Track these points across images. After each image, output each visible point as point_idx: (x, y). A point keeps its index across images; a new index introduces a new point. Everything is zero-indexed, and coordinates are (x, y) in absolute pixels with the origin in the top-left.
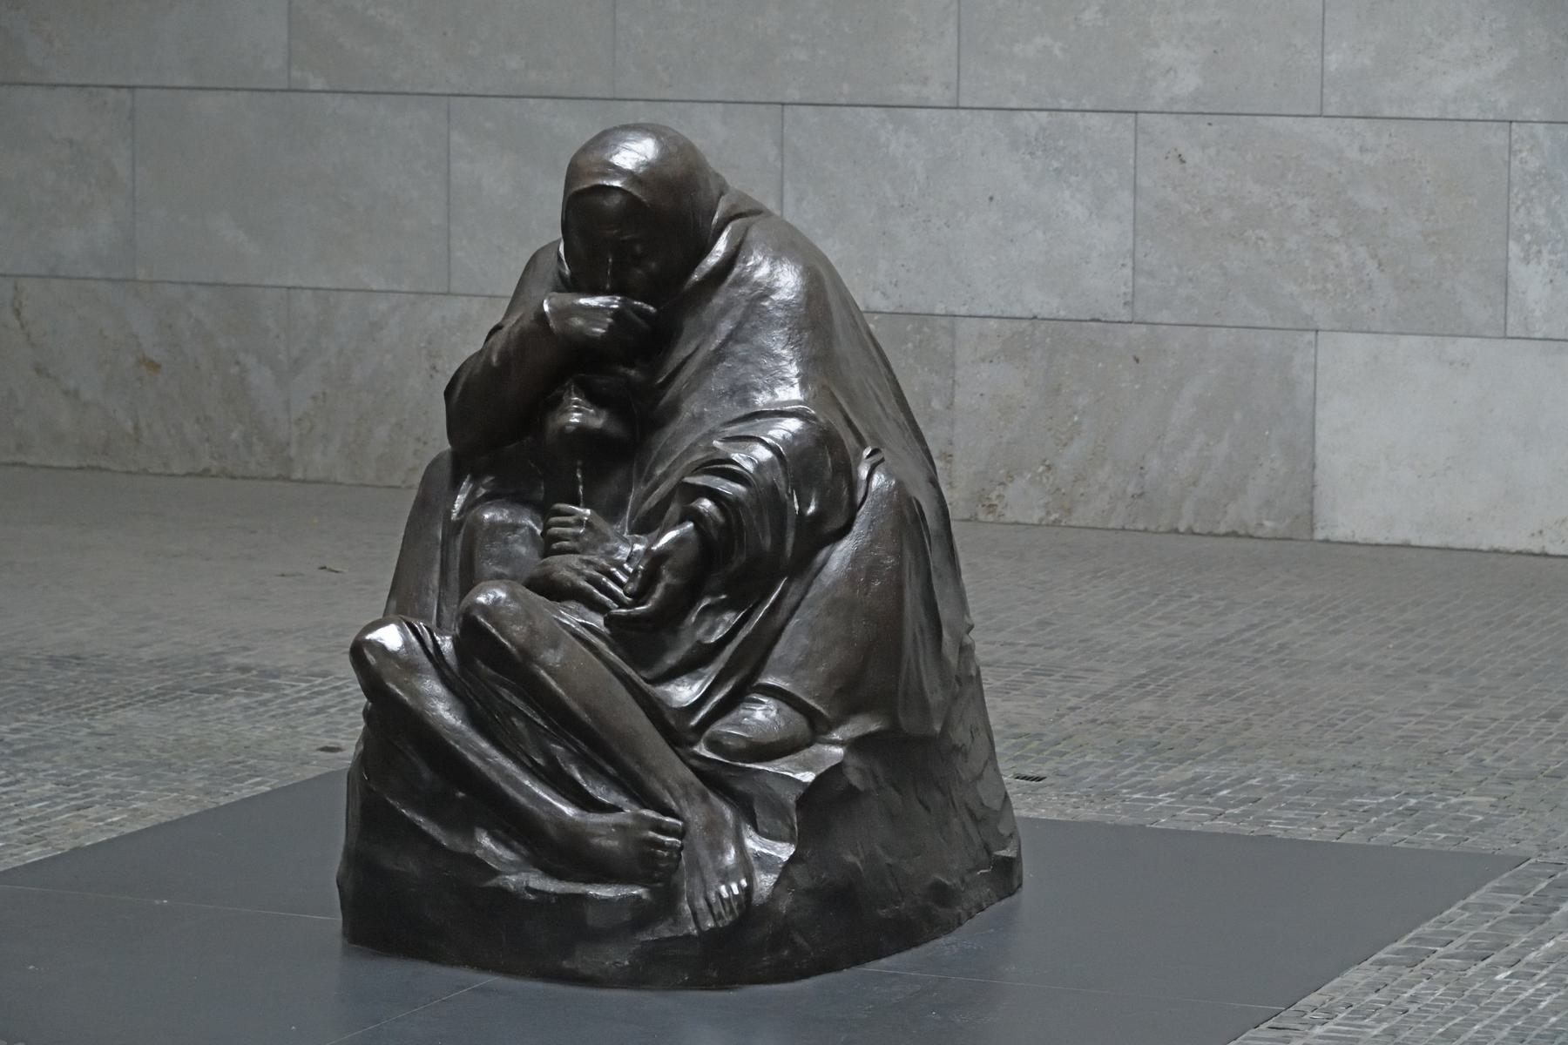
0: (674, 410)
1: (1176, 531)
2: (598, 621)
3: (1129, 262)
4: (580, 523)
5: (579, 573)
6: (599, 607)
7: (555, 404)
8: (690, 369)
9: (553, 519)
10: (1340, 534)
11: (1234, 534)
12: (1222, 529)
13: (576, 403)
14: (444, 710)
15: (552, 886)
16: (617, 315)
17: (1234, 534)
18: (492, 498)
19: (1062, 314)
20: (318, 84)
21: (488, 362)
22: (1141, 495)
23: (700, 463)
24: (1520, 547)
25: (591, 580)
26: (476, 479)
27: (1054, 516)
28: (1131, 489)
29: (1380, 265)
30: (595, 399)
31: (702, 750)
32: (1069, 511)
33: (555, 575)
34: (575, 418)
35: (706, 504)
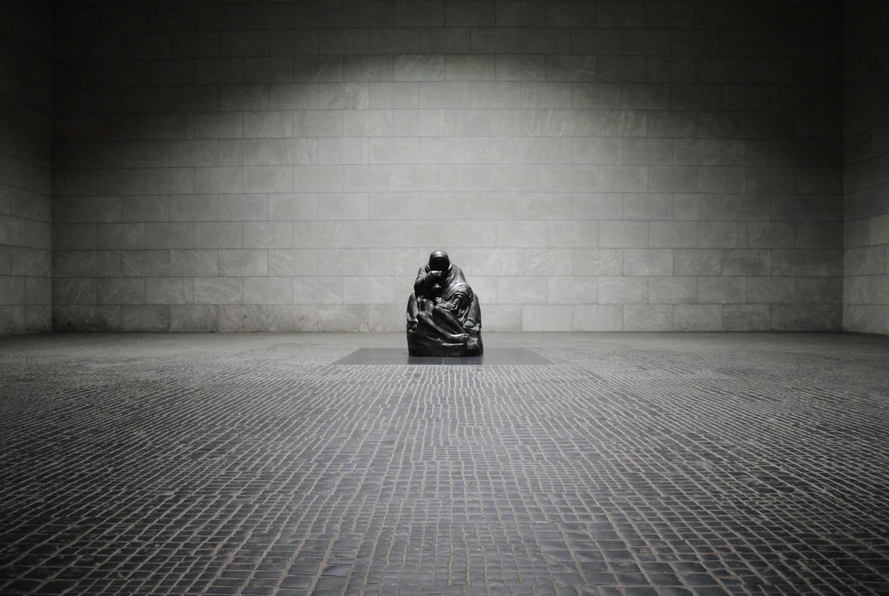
0: (448, 286)
7: (434, 285)
8: (450, 281)
14: (431, 322)
15: (451, 345)
18: (423, 298)
20: (272, 275)
21: (423, 280)
26: (420, 296)
30: (439, 284)
34: (438, 286)
35: (459, 296)
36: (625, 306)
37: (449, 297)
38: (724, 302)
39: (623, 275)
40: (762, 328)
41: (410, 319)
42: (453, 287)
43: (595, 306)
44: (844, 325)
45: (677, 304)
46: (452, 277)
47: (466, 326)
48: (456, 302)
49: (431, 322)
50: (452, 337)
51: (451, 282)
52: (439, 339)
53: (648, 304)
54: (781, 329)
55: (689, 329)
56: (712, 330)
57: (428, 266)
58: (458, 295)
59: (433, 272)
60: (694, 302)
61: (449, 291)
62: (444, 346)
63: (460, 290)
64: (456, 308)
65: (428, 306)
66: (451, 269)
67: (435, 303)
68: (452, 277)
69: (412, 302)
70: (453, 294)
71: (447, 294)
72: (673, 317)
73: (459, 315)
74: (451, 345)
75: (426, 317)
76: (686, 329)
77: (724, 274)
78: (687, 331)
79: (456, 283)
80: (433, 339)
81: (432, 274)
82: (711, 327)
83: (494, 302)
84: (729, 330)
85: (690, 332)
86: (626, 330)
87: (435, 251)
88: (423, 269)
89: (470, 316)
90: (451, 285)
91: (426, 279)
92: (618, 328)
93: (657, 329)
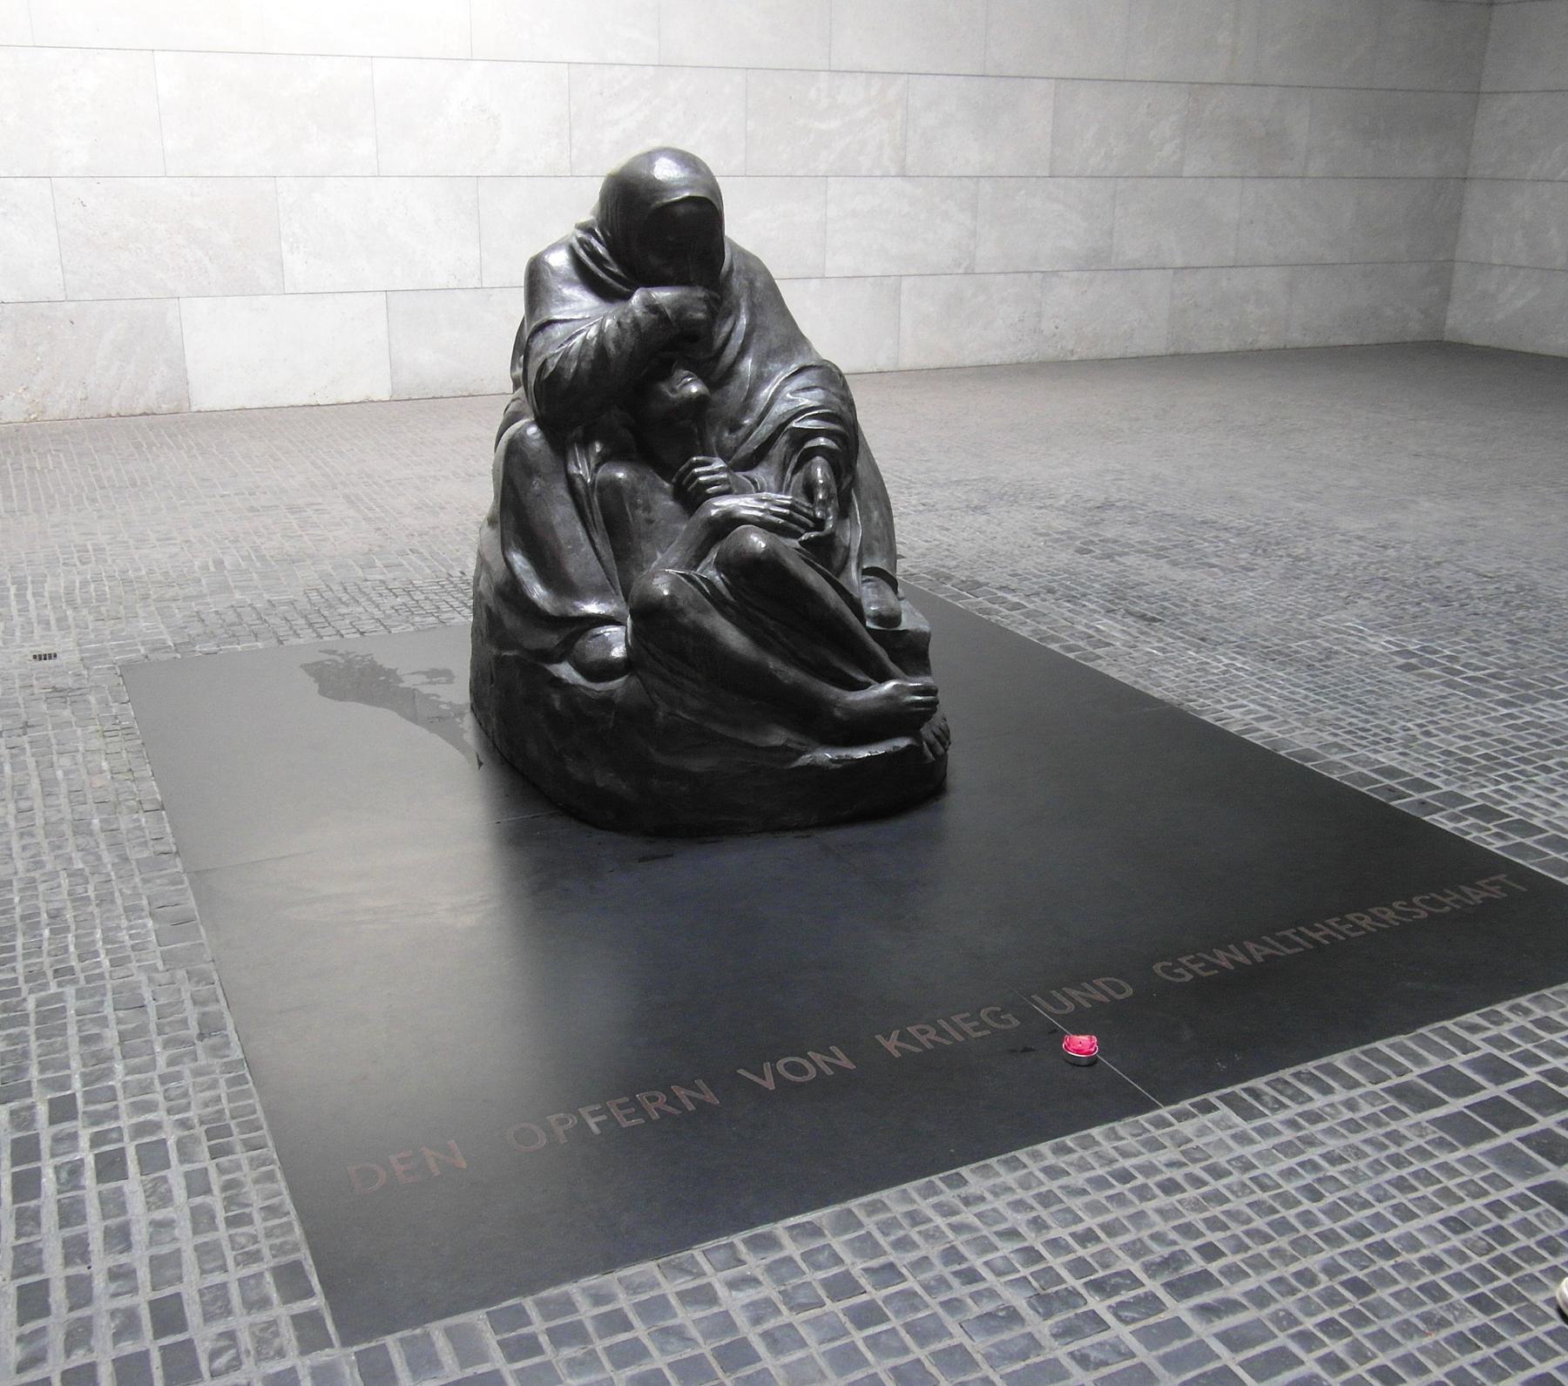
0: (731, 371)
1: (111, 416)
2: (795, 543)
3: (60, 268)
4: (721, 470)
5: (761, 510)
6: (797, 535)
9: (696, 470)
10: (206, 406)
11: (145, 414)
12: (138, 411)
13: (689, 376)
14: (732, 637)
16: (705, 300)
17: (145, 414)
18: (604, 459)
19: (21, 299)
21: (601, 349)
22: (86, 399)
23: (795, 412)
24: (304, 403)
25: (776, 514)
26: (585, 444)
27: (32, 417)
28: (80, 395)
29: (210, 259)
31: (869, 624)
32: (43, 412)
33: (737, 515)
34: (694, 389)
35: (822, 441)
36: (906, 283)
37: (751, 446)
38: (1179, 262)
39: (903, 175)
40: (1265, 341)
41: (538, 592)
42: (761, 379)
43: (814, 284)
44: (1450, 322)
45: (1055, 273)
46: (743, 321)
47: (879, 618)
48: (826, 487)
49: (732, 637)
50: (847, 709)
51: (743, 352)
52: (778, 737)
53: (969, 272)
54: (1308, 341)
55: (1083, 352)
56: (1141, 352)
57: (601, 250)
58: (813, 434)
59: (662, 295)
60: (1097, 262)
61: (746, 407)
62: (810, 768)
63: (805, 400)
64: (830, 526)
65: (648, 508)
66: (731, 269)
67: (691, 497)
68: (743, 321)
69: (537, 485)
70: (781, 428)
71: (735, 426)
72: (1039, 315)
73: (837, 563)
74: (862, 753)
75: (704, 611)
76: (1072, 352)
77: (1187, 171)
78: (1075, 358)
79: (770, 355)
80: (746, 737)
81: (653, 308)
82: (1140, 346)
83: (474, 283)
84: (1183, 350)
85: (1084, 363)
86: (907, 362)
87: (650, 157)
88: (559, 260)
89: (871, 553)
90: (748, 365)
91: (618, 344)
92: (882, 362)
93: (992, 357)
